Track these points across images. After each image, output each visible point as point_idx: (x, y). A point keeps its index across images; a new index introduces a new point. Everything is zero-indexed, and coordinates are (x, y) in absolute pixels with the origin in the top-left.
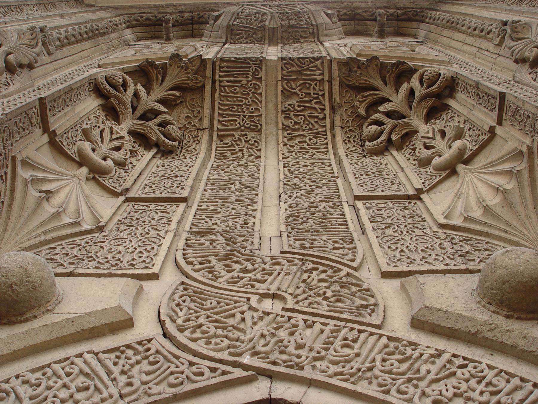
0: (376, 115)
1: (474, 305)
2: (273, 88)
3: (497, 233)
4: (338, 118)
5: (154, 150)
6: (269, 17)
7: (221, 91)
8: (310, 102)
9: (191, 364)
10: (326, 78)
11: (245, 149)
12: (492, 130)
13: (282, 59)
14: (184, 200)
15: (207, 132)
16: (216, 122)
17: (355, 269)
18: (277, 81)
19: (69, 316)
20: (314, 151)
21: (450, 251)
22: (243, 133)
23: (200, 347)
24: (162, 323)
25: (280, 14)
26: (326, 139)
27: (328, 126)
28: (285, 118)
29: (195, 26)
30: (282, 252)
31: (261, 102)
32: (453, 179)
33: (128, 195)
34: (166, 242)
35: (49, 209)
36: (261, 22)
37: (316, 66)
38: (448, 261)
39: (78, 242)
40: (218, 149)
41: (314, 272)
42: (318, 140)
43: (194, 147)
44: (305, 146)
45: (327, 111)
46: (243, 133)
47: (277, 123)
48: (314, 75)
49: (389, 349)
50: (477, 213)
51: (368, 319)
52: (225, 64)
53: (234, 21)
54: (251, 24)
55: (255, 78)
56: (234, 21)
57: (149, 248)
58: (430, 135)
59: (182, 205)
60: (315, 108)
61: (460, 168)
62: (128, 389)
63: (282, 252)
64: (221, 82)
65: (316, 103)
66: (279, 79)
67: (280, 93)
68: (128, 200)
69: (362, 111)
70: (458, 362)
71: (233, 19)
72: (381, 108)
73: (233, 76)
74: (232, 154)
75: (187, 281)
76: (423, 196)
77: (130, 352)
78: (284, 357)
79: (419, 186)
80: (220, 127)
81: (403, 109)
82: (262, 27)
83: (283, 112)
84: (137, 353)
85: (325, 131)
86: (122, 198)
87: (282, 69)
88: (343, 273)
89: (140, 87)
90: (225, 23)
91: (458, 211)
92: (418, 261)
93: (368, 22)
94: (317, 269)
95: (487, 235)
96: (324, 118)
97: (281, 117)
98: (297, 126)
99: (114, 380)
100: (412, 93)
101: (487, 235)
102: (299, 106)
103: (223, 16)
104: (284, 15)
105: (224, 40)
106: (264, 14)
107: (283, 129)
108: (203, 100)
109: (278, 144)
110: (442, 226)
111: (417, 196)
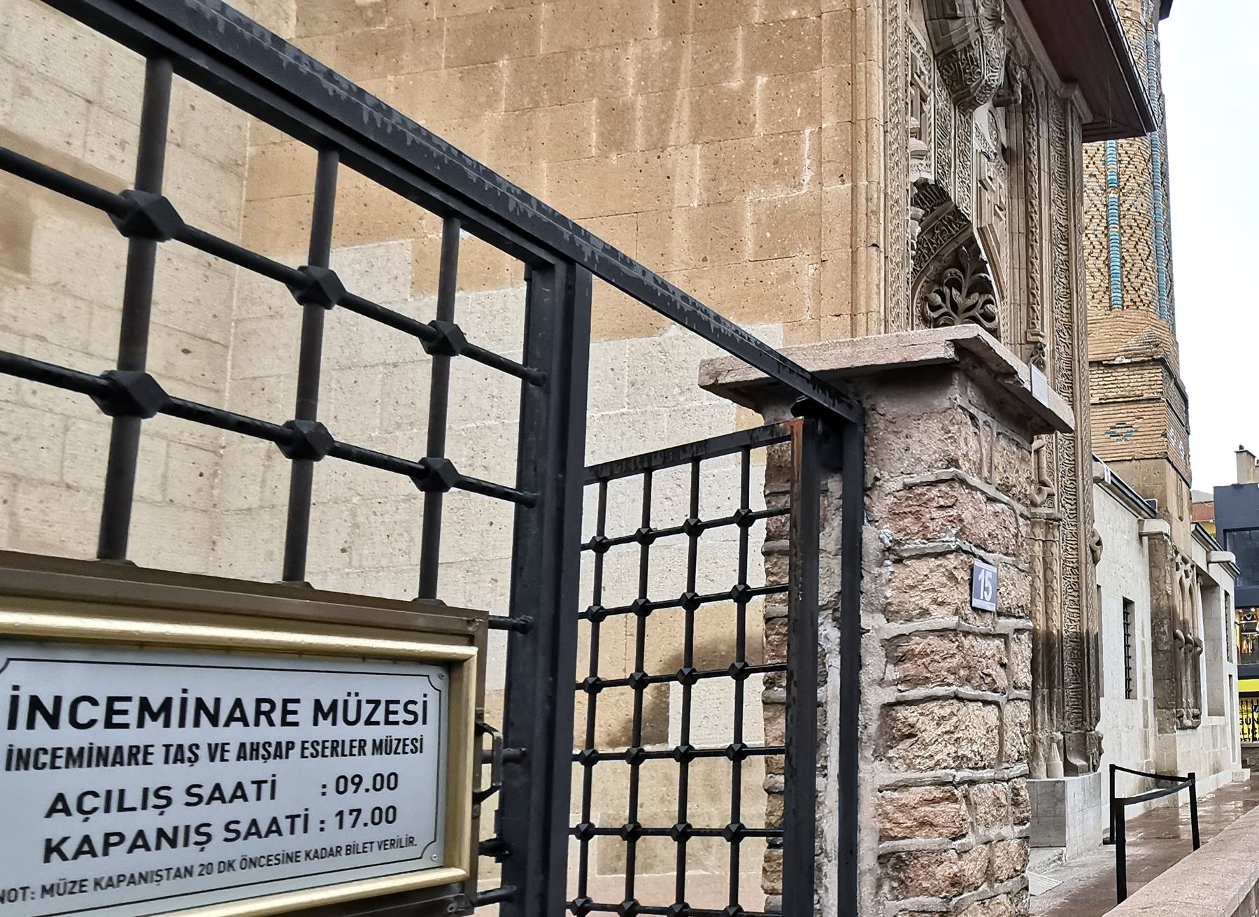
25: (986, 84)
37: (960, 225)
48: (954, 229)
53: (961, 50)
54: (965, 73)
72: (954, 292)
81: (960, 309)
102: (927, 244)
106: (980, 73)
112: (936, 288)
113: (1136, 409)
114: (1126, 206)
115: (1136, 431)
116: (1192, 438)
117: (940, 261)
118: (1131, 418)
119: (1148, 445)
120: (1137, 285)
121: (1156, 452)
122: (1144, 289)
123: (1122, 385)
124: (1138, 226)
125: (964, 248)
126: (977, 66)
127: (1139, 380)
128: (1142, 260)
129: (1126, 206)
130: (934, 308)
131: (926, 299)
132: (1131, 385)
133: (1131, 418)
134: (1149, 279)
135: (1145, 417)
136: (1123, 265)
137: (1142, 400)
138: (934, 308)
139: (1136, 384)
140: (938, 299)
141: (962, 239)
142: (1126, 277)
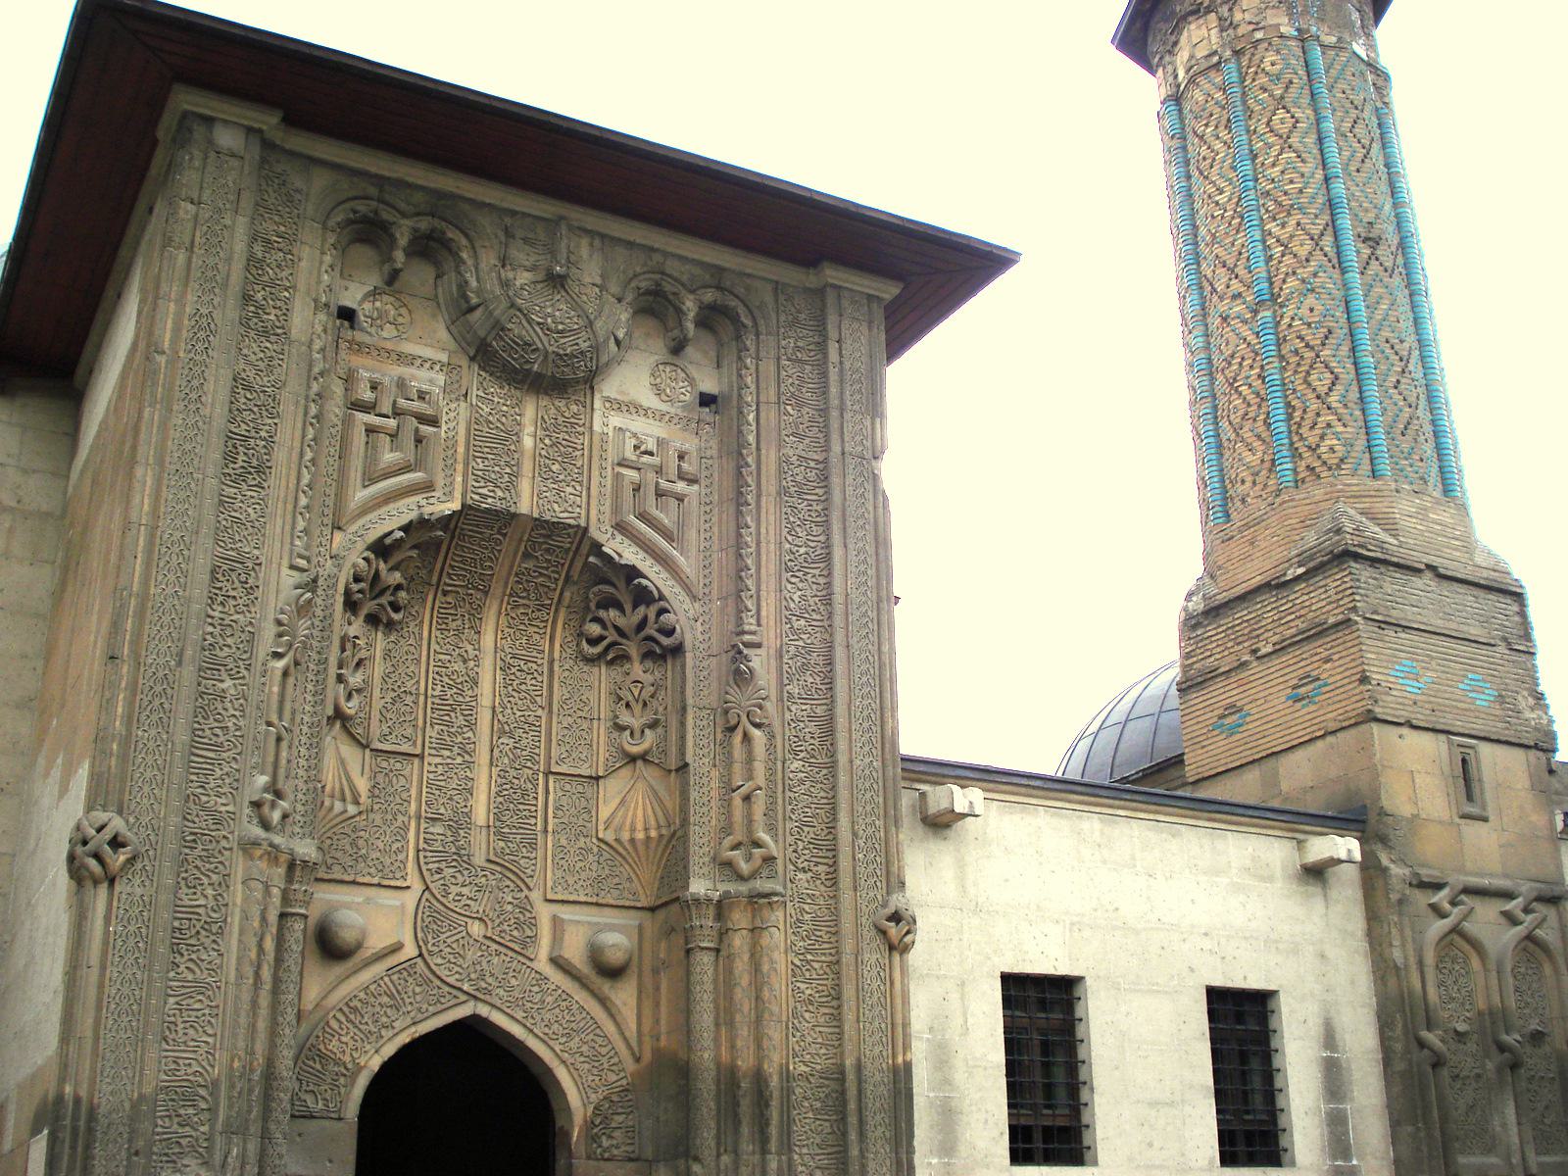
0: (605, 614)
1: (585, 959)
2: (514, 543)
3: (630, 860)
4: (567, 594)
5: (381, 628)
6: (542, 358)
7: (459, 538)
8: (547, 569)
9: (439, 988)
10: (574, 548)
11: (467, 616)
12: (670, 771)
13: (536, 519)
14: (417, 756)
15: (434, 588)
16: (444, 574)
17: (530, 889)
18: (521, 540)
19: (374, 951)
20: (532, 629)
21: (595, 875)
22: (470, 591)
23: (443, 973)
24: (419, 947)
25: (558, 354)
26: (548, 614)
27: (555, 601)
28: (517, 582)
29: (431, 243)
30: (489, 861)
31: (497, 559)
32: (631, 765)
33: (373, 746)
34: (411, 835)
35: (327, 803)
36: (527, 362)
37: (568, 534)
38: (589, 890)
39: (346, 831)
40: (442, 611)
41: (506, 890)
42: (539, 614)
43: (416, 608)
44: (527, 622)
45: (560, 583)
46: (470, 591)
47: (506, 583)
49: (534, 982)
50: (626, 836)
51: (527, 954)
52: (472, 512)
53: (495, 339)
55: (499, 533)
56: (495, 339)
57: (399, 845)
58: (636, 694)
59: (416, 761)
60: (550, 577)
61: (640, 763)
62: (409, 1008)
63: (489, 861)
64: (462, 529)
65: (553, 572)
66: (525, 538)
67: (520, 553)
68: (372, 750)
69: (592, 605)
70: (564, 996)
71: (494, 333)
73: (477, 526)
74: (453, 620)
75: (427, 895)
76: (601, 782)
77: (405, 973)
78: (484, 985)
79: (601, 774)
80: (448, 581)
82: (527, 370)
83: (517, 575)
84: (410, 975)
85: (551, 605)
86: (367, 751)
87: (532, 530)
88: (523, 895)
89: (382, 565)
90: (482, 333)
91: (617, 821)
92: (571, 889)
93: (671, 309)
94: (508, 886)
95: (624, 858)
96: (555, 590)
97: (513, 579)
98: (524, 594)
99: (402, 999)
100: (645, 620)
101: (624, 858)
102: (535, 572)
103: (480, 309)
104: (562, 359)
105: (472, 354)
106: (537, 349)
107: (511, 595)
108: (438, 554)
109: (500, 613)
110: (599, 839)
111: (597, 778)
112: (589, 617)
113: (1320, 648)
114: (1286, 320)
115: (1326, 685)
116: (1541, 660)
117: (575, 583)
118: (1316, 665)
119: (1344, 704)
120: (1313, 440)
121: (1355, 713)
122: (1328, 442)
123: (1303, 612)
124: (1307, 346)
125: (591, 559)
126: (526, 344)
127: (1323, 596)
128: (1318, 397)
129: (1286, 320)
130: (593, 642)
131: (580, 635)
132: (1314, 608)
133: (1316, 665)
134: (1336, 423)
135: (1335, 657)
136: (1290, 417)
137: (1327, 629)
138: (593, 642)
139: (1319, 605)
140: (595, 629)
141: (585, 548)
142: (1297, 433)
